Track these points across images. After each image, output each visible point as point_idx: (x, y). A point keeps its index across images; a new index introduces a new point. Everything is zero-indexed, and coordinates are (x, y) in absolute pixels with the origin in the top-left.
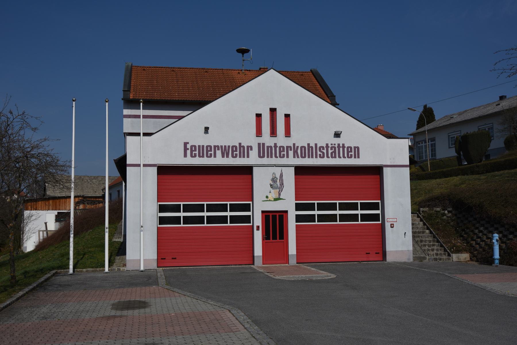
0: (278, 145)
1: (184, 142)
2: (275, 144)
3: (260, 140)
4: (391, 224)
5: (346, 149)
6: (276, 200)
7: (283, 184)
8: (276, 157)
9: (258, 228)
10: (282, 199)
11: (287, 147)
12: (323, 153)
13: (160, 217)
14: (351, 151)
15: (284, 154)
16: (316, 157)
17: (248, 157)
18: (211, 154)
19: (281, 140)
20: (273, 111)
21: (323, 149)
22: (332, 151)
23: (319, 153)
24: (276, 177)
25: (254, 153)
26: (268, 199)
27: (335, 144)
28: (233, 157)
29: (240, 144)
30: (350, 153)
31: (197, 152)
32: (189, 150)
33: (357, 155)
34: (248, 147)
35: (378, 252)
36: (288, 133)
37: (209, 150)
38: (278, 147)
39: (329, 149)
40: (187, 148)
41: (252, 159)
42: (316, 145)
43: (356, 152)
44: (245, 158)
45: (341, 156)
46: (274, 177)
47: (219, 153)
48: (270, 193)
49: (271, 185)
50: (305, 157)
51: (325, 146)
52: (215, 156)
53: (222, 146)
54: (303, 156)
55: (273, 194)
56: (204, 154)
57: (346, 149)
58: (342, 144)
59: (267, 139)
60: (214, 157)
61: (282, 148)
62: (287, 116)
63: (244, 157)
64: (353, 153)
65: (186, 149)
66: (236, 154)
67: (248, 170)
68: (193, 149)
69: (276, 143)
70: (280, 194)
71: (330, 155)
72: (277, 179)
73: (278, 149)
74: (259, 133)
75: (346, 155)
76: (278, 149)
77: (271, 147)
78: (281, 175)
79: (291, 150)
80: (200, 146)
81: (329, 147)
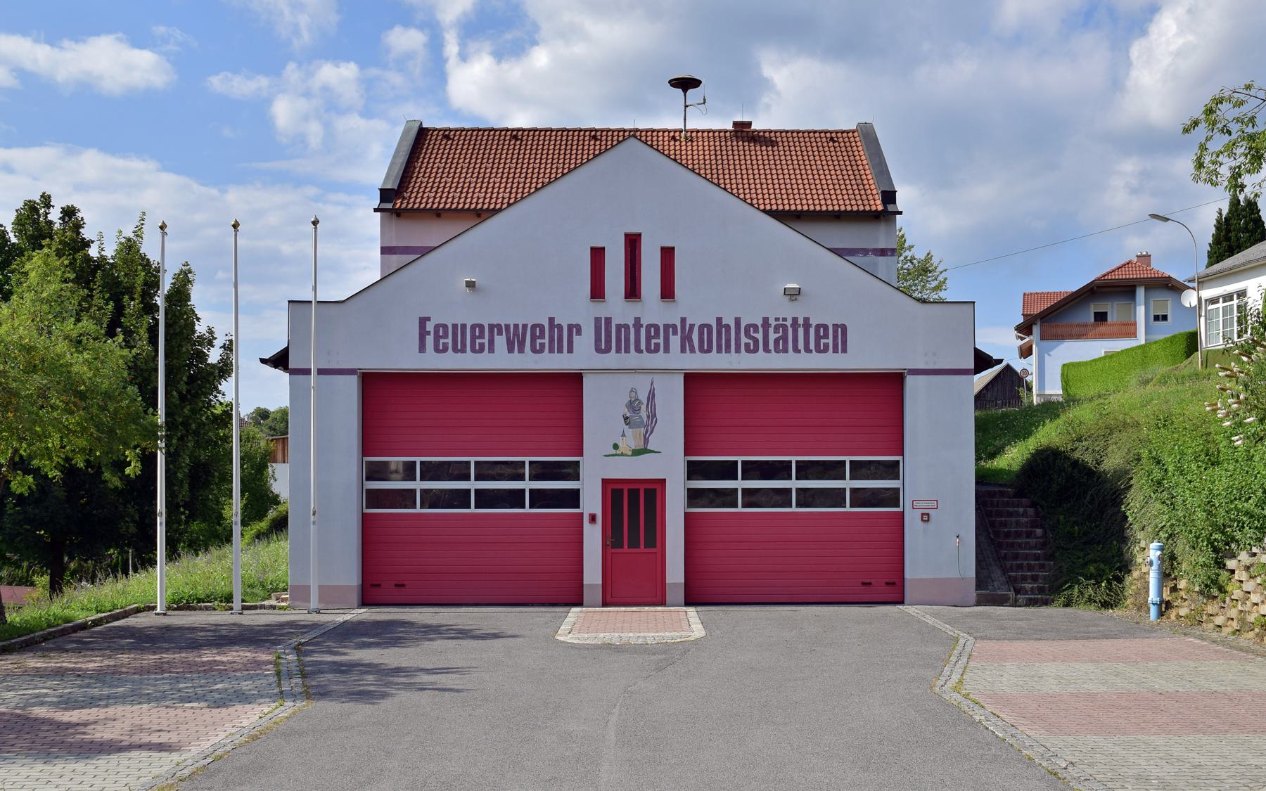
0: (644, 322)
1: (420, 318)
2: (636, 318)
3: (601, 310)
4: (923, 514)
5: (812, 331)
6: (636, 453)
7: (654, 415)
8: (638, 350)
9: (593, 518)
10: (653, 452)
11: (666, 327)
12: (756, 341)
13: (368, 491)
14: (826, 336)
15: (484, 343)
16: (738, 350)
17: (570, 350)
18: (482, 345)
19: (652, 308)
20: (633, 243)
21: (756, 330)
22: (777, 335)
23: (744, 340)
24: (640, 398)
25: (584, 342)
26: (618, 452)
27: (786, 319)
28: (534, 350)
29: (551, 320)
30: (823, 341)
31: (449, 341)
32: (429, 335)
33: (841, 345)
34: (570, 327)
35: (892, 581)
36: (668, 292)
37: (477, 334)
38: (644, 326)
39: (771, 330)
40: (427, 330)
41: (582, 356)
42: (738, 321)
43: (838, 337)
44: (562, 353)
45: (770, 348)
46: (633, 399)
47: (500, 341)
48: (622, 436)
49: (626, 418)
50: (709, 350)
51: (759, 323)
52: (492, 350)
53: (507, 327)
54: (706, 348)
55: (631, 441)
56: (466, 345)
57: (812, 331)
58: (804, 318)
59: (616, 306)
60: (489, 352)
61: (653, 329)
62: (668, 254)
63: (560, 350)
64: (830, 341)
65: (423, 334)
66: (542, 345)
67: (574, 381)
68: (441, 334)
69: (639, 318)
70: (646, 440)
71: (771, 346)
72: (641, 403)
73: (643, 331)
74: (597, 292)
75: (812, 346)
76: (643, 331)
77: (627, 327)
78: (651, 395)
79: (675, 333)
80: (457, 325)
81: (770, 326)
